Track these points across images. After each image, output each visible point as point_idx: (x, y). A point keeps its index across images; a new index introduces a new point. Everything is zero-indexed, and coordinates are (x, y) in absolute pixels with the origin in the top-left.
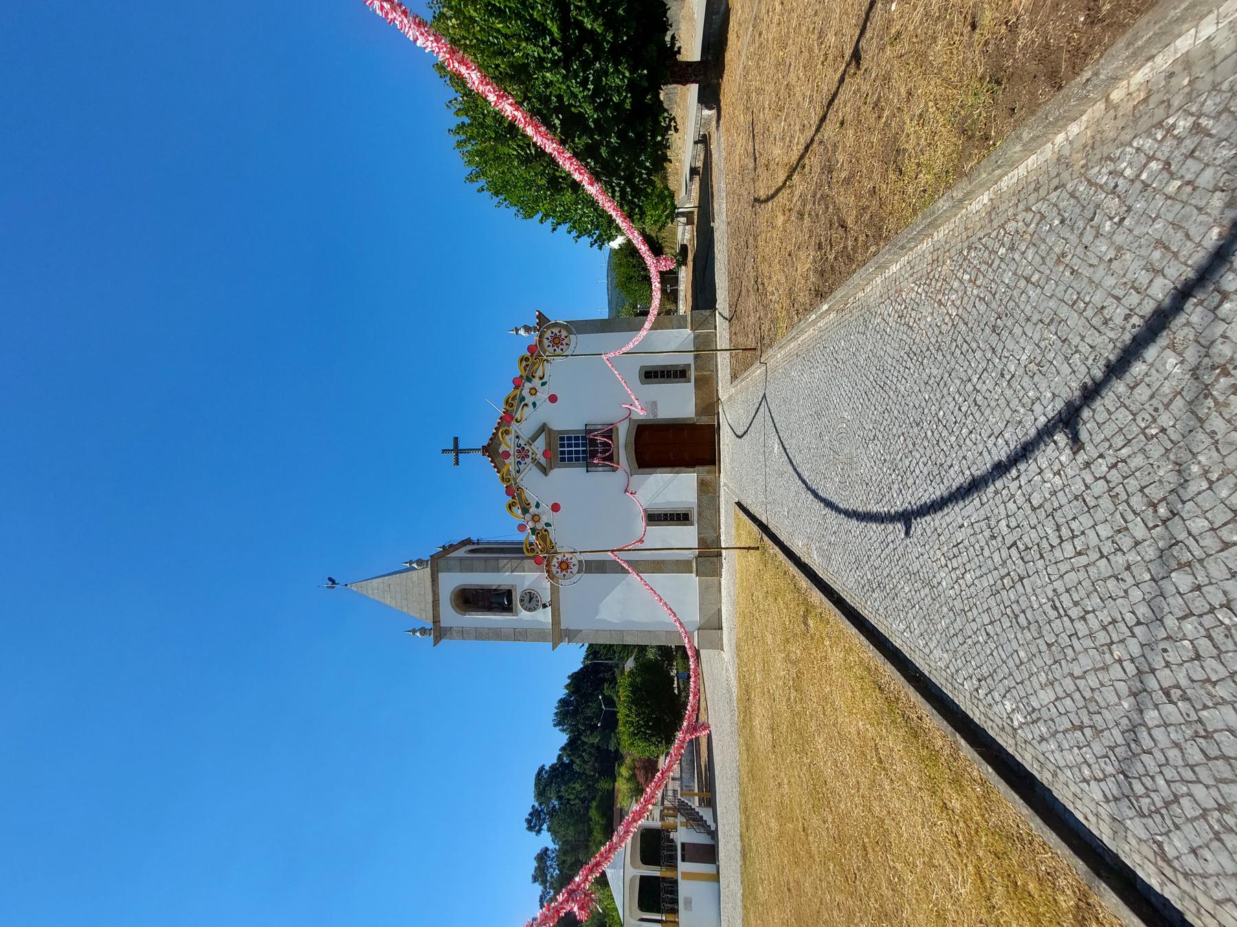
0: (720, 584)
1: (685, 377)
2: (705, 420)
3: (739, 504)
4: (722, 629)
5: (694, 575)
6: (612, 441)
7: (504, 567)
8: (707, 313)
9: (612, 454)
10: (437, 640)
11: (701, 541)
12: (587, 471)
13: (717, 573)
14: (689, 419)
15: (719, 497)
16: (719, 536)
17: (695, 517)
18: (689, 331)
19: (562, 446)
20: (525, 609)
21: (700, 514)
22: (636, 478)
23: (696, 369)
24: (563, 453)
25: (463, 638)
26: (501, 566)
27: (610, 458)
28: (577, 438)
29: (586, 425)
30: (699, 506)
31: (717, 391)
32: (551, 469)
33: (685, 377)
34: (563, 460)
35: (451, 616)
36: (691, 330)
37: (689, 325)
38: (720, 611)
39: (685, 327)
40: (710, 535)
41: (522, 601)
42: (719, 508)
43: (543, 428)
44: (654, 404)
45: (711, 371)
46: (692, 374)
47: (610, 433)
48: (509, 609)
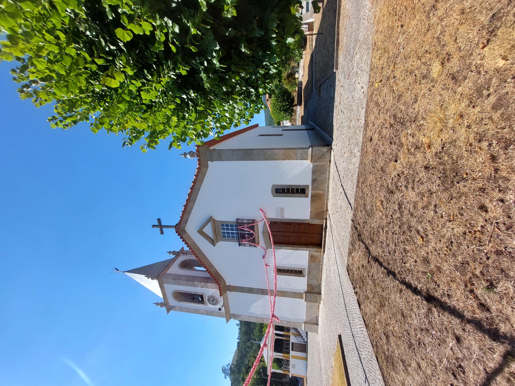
0: (319, 306)
1: (304, 193)
2: (316, 222)
3: (340, 337)
4: (318, 325)
5: (304, 300)
6: (254, 231)
7: (197, 285)
8: (325, 149)
9: (254, 239)
10: (168, 311)
11: (309, 285)
12: (240, 245)
13: (317, 301)
14: (306, 220)
15: (322, 265)
16: (320, 285)
17: (306, 273)
18: (309, 162)
19: (224, 229)
20: (211, 304)
21: (309, 272)
22: (270, 251)
23: (312, 189)
24: (224, 233)
25: (181, 311)
26: (195, 284)
27: (253, 241)
28: (232, 226)
29: (237, 220)
30: (309, 268)
31: (327, 204)
32: (217, 242)
33: (304, 193)
34: (224, 236)
35: (172, 302)
36: (311, 161)
37: (310, 158)
38: (317, 317)
39: (307, 159)
40: (315, 283)
41: (208, 300)
42: (322, 271)
43: (210, 219)
44: (282, 210)
45: (324, 191)
46: (310, 192)
47: (252, 224)
48: (202, 302)
